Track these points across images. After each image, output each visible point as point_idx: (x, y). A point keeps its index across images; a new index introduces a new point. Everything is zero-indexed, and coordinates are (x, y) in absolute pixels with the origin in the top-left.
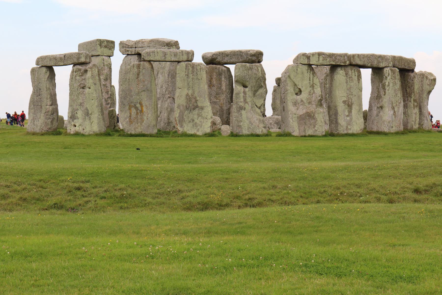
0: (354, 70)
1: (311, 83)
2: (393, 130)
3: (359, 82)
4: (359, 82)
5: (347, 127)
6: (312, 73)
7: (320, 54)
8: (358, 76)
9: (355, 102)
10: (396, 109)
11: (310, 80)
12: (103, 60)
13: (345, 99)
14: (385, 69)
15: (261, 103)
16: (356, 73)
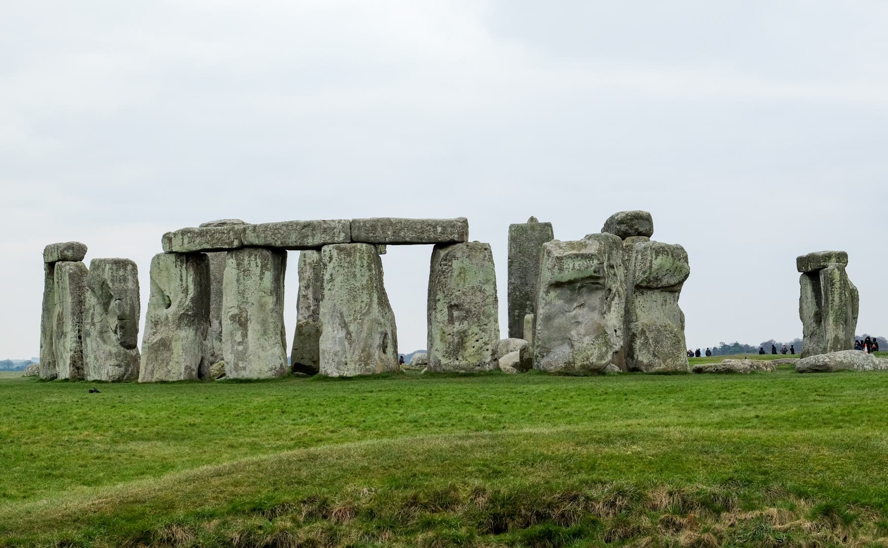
0: (256, 256)
1: (184, 285)
2: (350, 371)
3: (261, 279)
4: (261, 279)
5: (236, 365)
6: (184, 266)
7: (184, 232)
8: (262, 267)
9: (252, 317)
10: (352, 328)
11: (181, 280)
12: (305, 256)
13: (235, 311)
14: (324, 248)
15: (115, 325)
16: (259, 261)
